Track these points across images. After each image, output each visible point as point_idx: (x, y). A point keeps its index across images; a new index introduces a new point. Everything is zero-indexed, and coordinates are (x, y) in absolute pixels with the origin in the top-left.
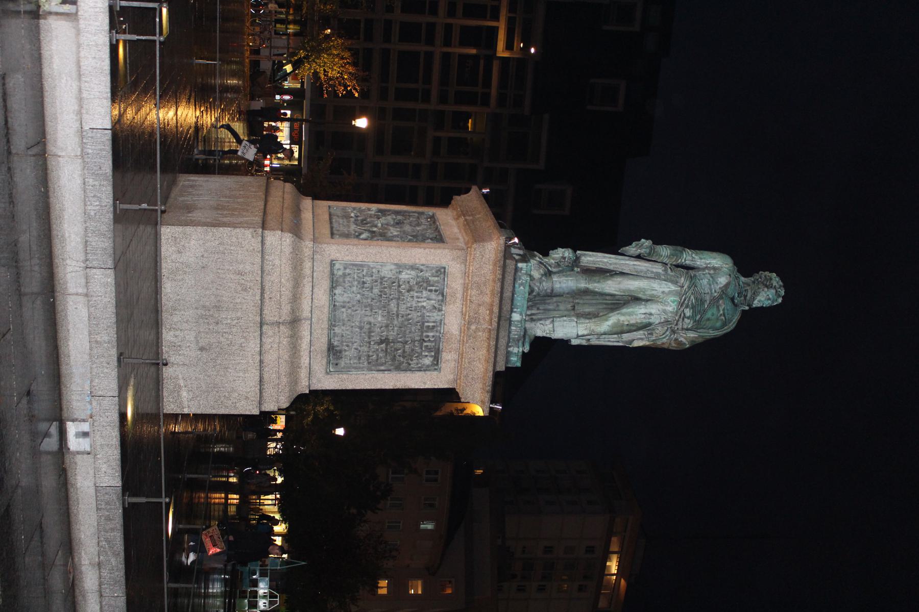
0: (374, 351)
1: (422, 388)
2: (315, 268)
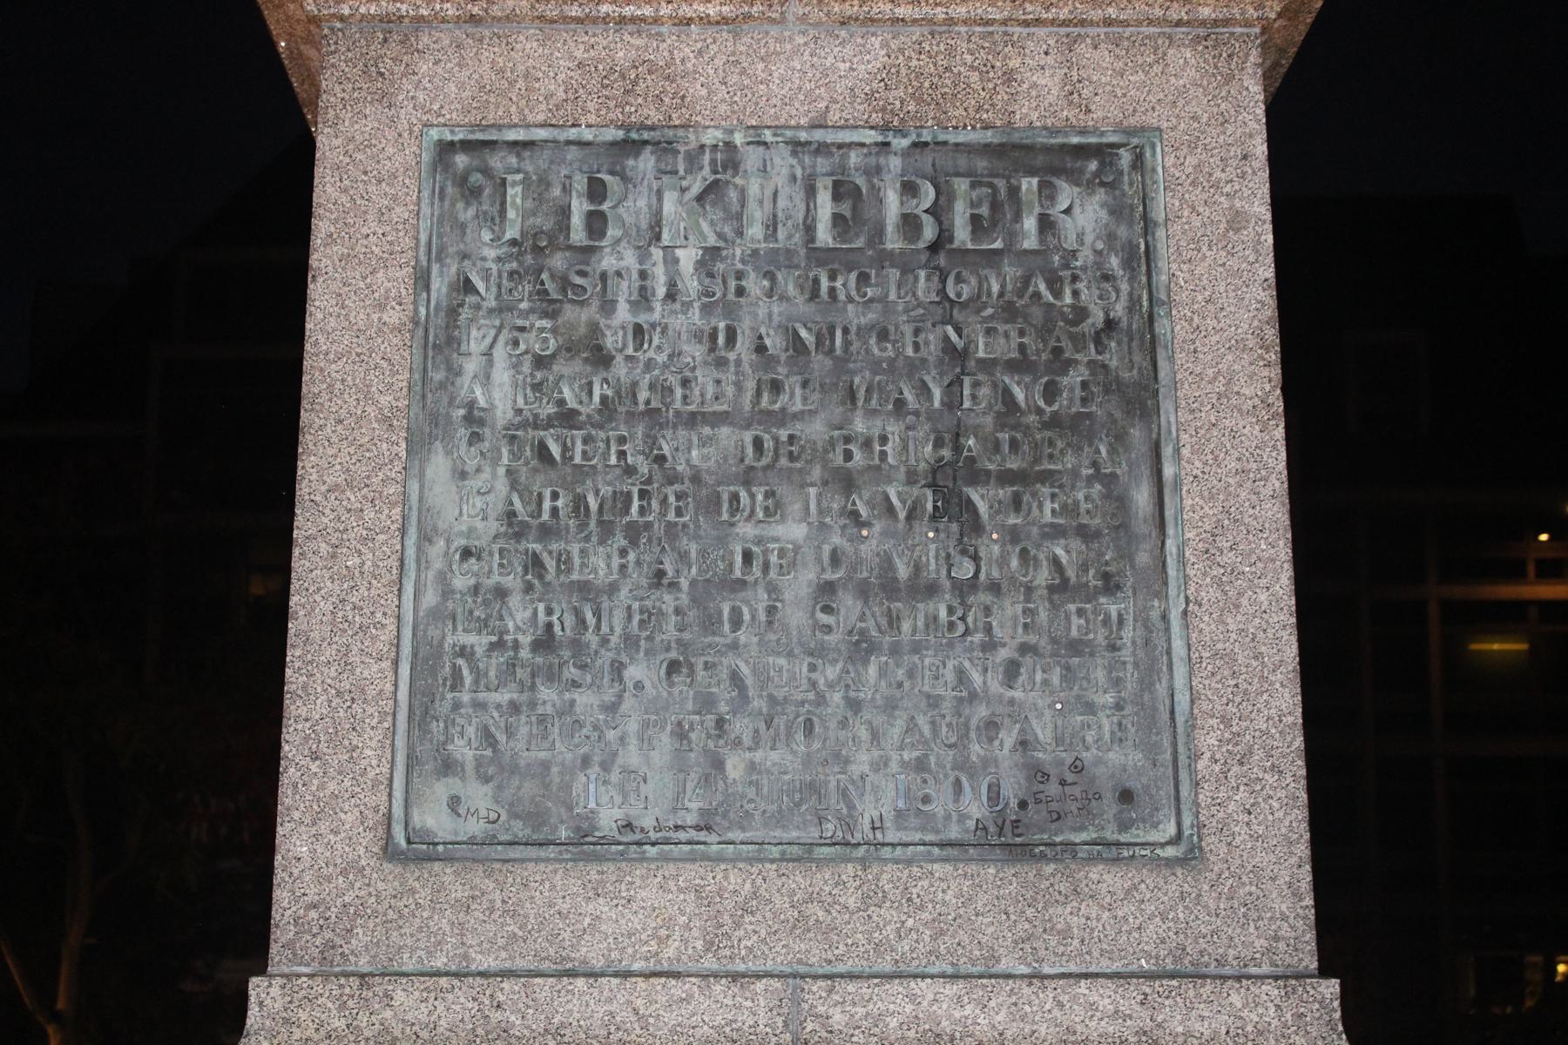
0: (1024, 553)
1: (1270, 238)
2: (439, 962)
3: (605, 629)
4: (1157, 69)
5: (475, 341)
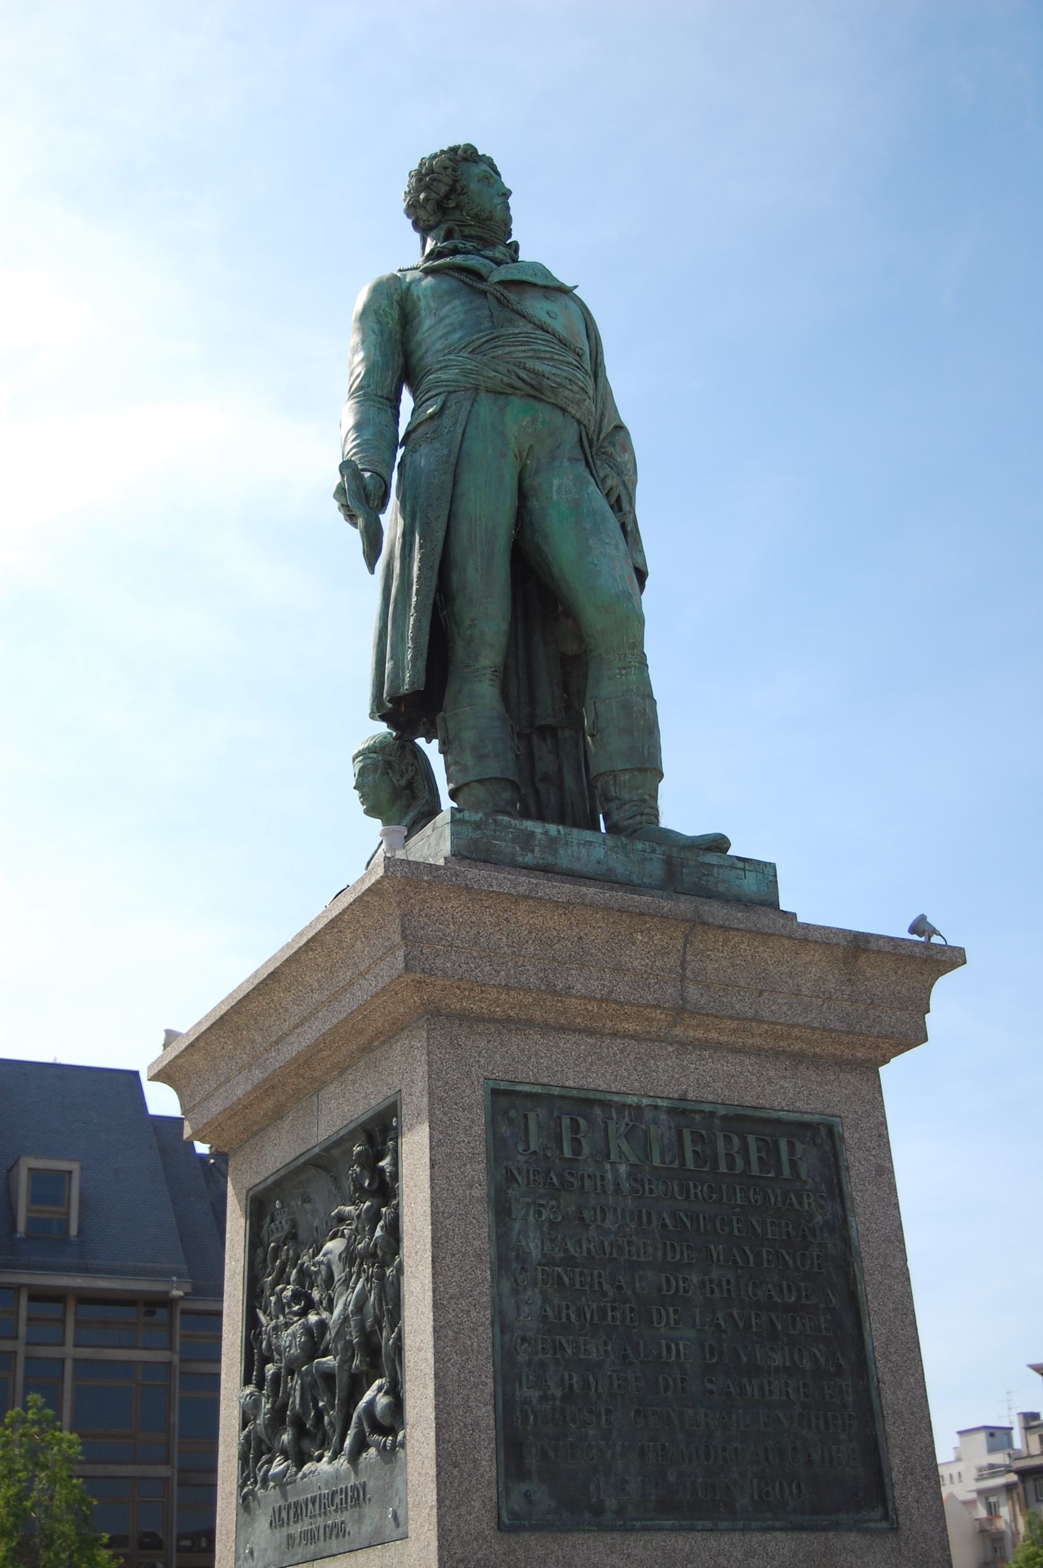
3: (600, 1390)
4: (836, 1084)
5: (518, 1211)
